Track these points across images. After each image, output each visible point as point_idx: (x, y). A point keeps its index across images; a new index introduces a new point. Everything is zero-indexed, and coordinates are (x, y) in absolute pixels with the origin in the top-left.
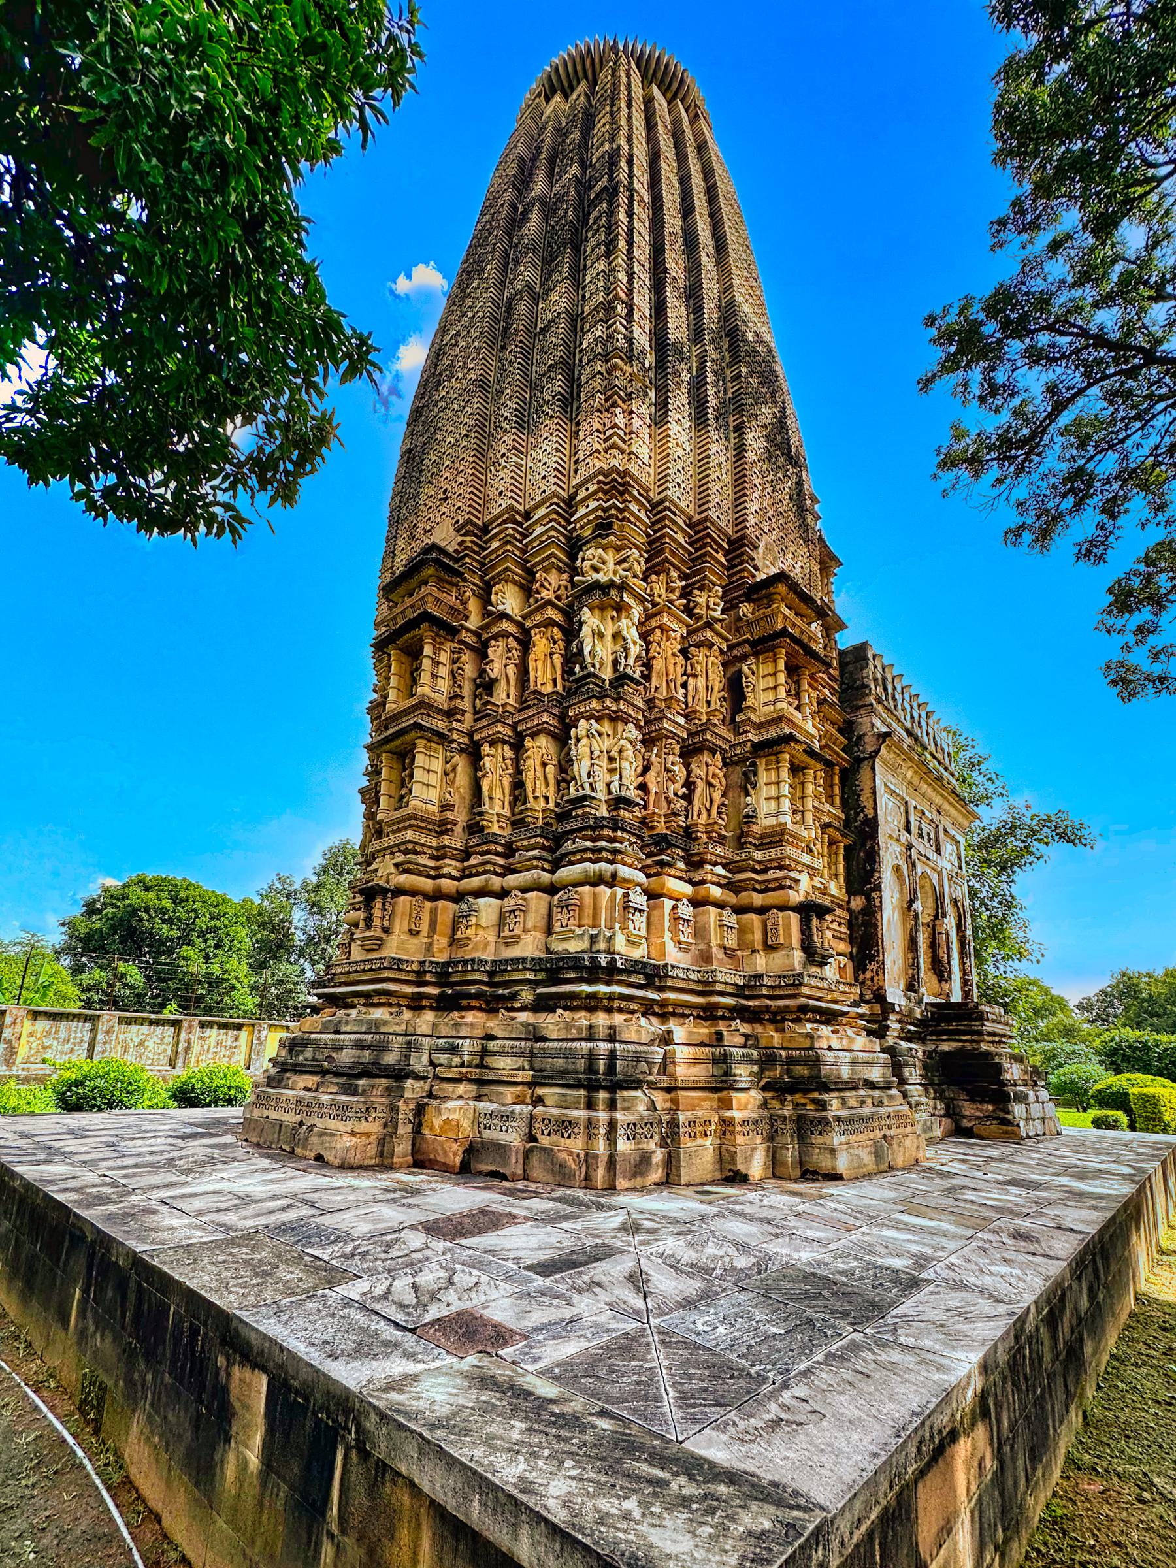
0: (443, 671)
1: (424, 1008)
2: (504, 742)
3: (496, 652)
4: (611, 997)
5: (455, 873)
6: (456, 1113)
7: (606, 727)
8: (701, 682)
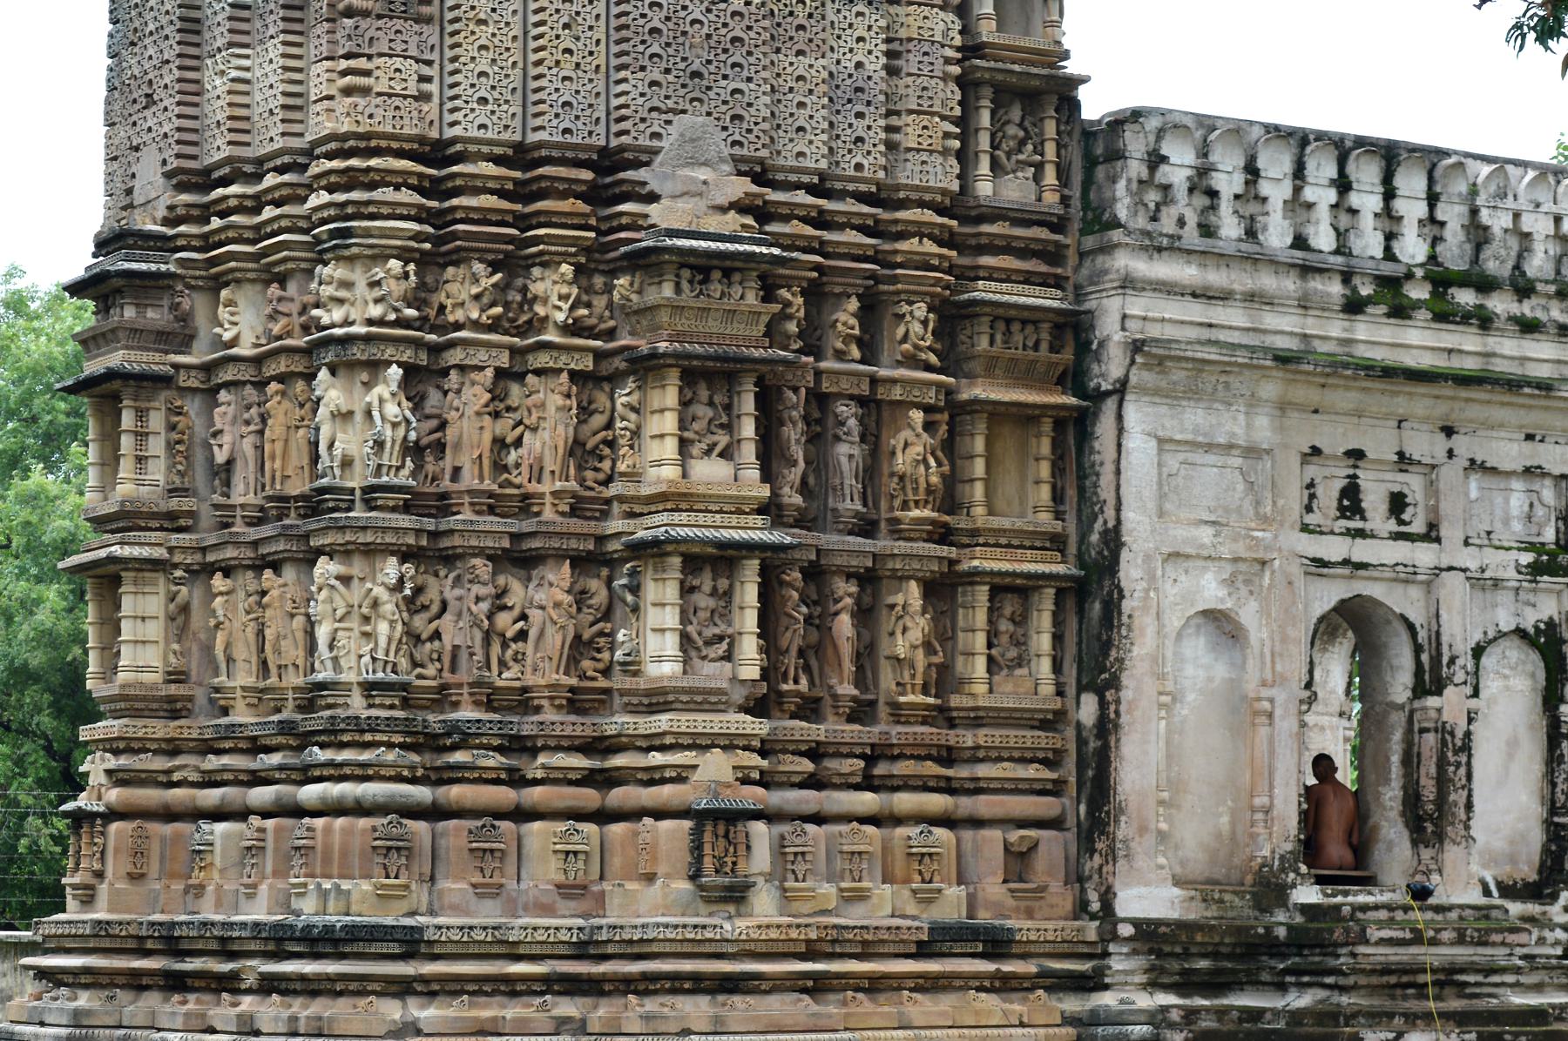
0: (156, 446)
1: (147, 988)
2: (248, 567)
4: (329, 978)
5: (194, 777)
7: (357, 567)
8: (545, 435)
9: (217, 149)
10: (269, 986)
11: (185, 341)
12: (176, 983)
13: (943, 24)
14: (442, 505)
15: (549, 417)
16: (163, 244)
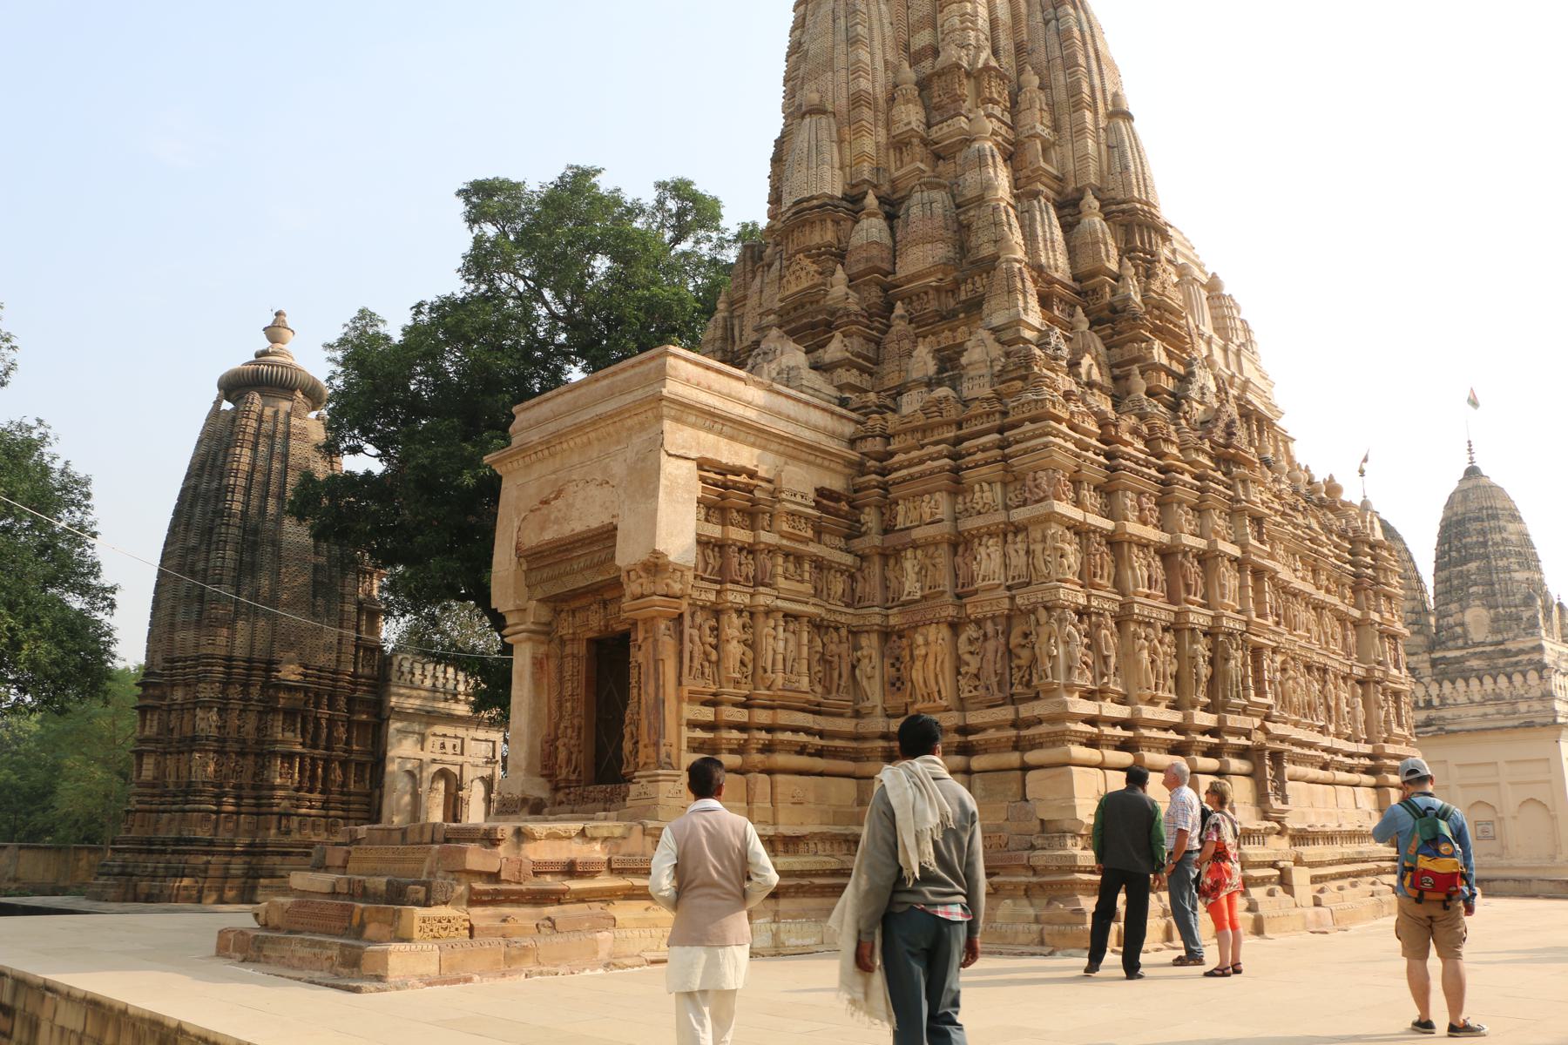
3: (174, 715)
6: (144, 886)
9: (177, 654)
10: (174, 852)
11: (163, 698)
12: (150, 852)
13: (353, 633)
14: (224, 740)
15: (251, 722)
16: (162, 675)
